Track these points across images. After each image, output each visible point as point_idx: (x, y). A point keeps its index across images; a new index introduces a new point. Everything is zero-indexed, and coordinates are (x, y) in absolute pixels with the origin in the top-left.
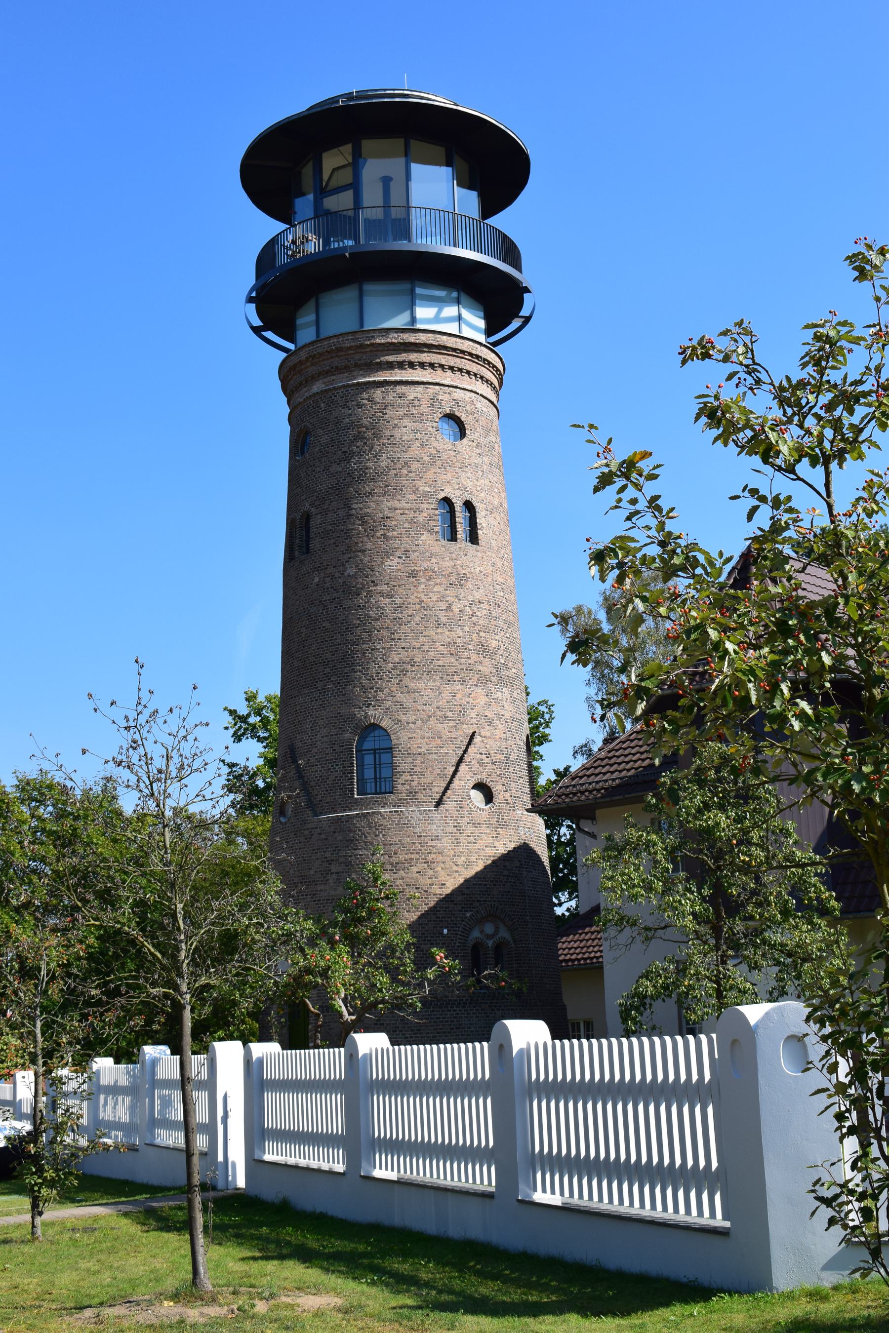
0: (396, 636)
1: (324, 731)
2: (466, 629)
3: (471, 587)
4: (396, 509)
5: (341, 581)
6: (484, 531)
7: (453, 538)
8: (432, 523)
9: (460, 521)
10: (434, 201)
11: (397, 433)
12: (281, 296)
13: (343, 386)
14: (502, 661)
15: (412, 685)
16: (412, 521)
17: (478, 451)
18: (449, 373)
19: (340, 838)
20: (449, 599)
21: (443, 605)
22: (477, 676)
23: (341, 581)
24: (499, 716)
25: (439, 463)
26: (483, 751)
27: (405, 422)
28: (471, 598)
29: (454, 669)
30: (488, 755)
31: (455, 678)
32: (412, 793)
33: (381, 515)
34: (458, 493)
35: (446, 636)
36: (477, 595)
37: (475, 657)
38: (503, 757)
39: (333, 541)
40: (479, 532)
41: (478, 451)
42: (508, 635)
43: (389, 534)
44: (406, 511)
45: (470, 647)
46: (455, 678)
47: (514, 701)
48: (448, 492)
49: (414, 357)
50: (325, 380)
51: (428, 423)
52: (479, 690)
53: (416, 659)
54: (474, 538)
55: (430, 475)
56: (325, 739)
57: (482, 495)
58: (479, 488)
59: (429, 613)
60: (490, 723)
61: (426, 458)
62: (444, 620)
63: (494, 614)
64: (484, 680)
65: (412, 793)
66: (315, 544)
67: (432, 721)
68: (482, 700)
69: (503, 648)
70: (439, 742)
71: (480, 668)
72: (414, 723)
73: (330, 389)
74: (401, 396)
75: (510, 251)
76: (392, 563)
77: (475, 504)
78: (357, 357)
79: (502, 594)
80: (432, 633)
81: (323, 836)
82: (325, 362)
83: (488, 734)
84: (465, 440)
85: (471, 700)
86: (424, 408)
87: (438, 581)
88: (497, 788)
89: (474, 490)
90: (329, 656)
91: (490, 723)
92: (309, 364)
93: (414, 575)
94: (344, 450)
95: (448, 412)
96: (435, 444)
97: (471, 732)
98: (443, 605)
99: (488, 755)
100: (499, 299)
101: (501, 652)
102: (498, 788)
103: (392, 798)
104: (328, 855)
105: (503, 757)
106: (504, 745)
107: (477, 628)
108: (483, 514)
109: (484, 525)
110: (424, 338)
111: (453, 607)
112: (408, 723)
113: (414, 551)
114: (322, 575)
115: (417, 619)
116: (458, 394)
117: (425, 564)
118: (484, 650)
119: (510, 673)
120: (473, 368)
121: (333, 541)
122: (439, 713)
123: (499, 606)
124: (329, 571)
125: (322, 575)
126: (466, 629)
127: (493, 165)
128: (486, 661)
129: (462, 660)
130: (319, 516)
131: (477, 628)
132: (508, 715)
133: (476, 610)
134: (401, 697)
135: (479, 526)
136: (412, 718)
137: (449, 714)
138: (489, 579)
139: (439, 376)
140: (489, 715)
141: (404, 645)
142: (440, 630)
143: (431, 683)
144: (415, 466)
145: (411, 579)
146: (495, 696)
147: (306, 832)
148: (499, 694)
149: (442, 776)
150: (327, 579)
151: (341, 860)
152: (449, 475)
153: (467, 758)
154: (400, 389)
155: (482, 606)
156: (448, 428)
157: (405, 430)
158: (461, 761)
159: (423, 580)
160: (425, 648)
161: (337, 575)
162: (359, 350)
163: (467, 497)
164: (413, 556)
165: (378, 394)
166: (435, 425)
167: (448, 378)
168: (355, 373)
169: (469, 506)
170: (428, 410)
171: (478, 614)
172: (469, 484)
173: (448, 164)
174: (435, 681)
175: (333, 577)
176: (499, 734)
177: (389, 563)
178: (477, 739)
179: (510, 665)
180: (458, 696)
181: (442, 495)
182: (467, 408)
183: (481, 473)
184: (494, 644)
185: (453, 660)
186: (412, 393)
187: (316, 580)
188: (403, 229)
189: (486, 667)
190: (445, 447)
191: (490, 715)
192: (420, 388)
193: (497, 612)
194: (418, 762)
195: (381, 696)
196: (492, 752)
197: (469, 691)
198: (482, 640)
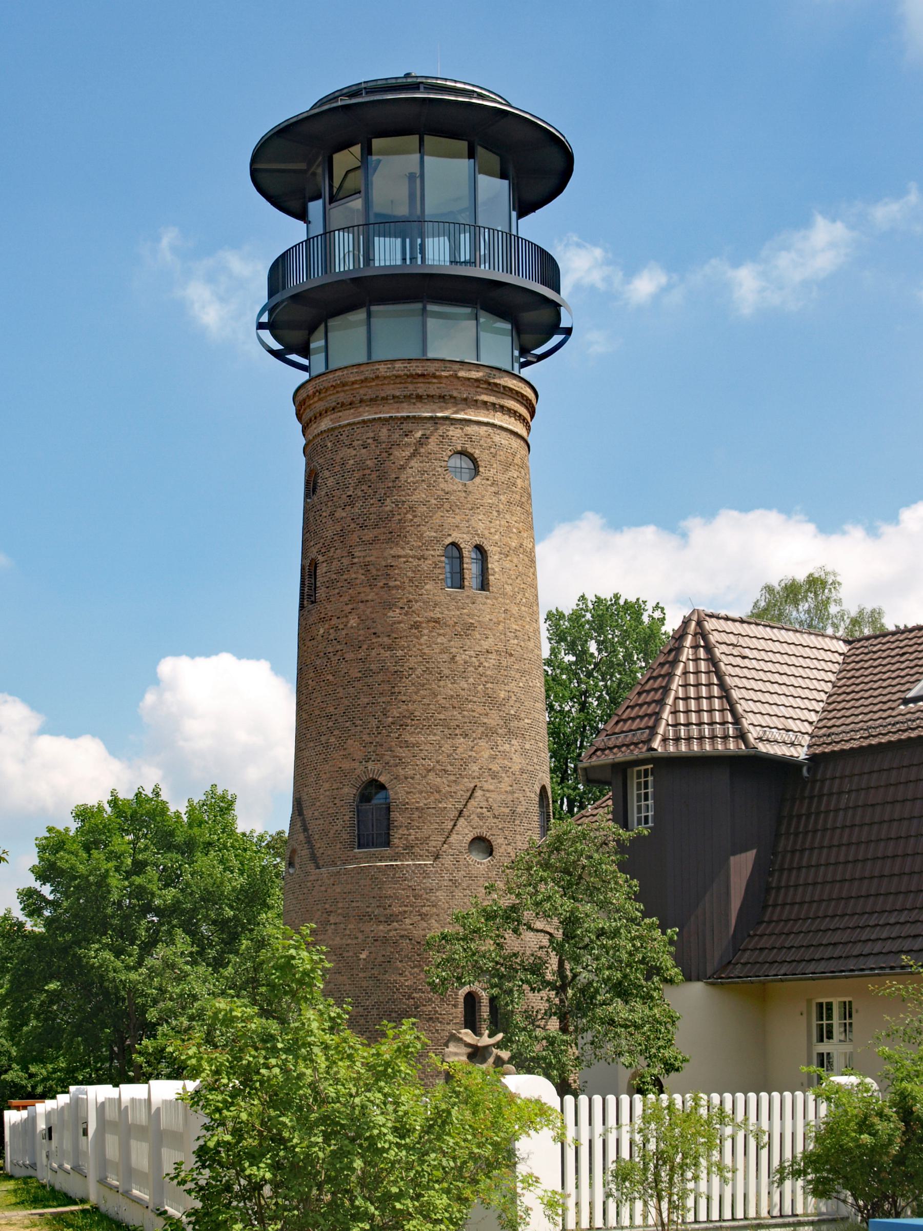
0: (396, 689)
1: (327, 786)
2: (471, 680)
3: (478, 636)
4: (399, 557)
5: (344, 632)
6: (497, 576)
7: (460, 584)
8: (438, 571)
13: (349, 424)
14: (512, 712)
17: (493, 489)
19: (338, 890)
20: (453, 650)
21: (446, 657)
22: (481, 729)
23: (344, 632)
24: (506, 769)
25: (447, 506)
26: (484, 804)
28: (478, 648)
29: (457, 723)
30: (490, 809)
31: (457, 732)
32: (409, 847)
33: (384, 563)
35: (449, 688)
36: (486, 645)
37: (480, 709)
38: (507, 810)
39: (337, 591)
40: (491, 578)
41: (493, 489)
42: (521, 684)
43: (391, 584)
44: (410, 559)
45: (475, 699)
46: (457, 732)
48: (456, 536)
50: (332, 417)
51: (436, 463)
53: (417, 714)
54: (484, 585)
55: (436, 520)
56: (328, 793)
57: (497, 537)
58: (493, 530)
59: (431, 665)
60: (494, 776)
61: (434, 501)
62: (447, 672)
63: (504, 664)
65: (409, 847)
66: (321, 593)
67: (431, 776)
68: (486, 754)
69: (514, 698)
71: (486, 720)
72: (412, 778)
73: (336, 428)
78: (362, 391)
79: (516, 641)
81: (323, 888)
82: (332, 397)
83: (492, 787)
84: (478, 480)
85: (474, 754)
87: (442, 631)
88: (498, 841)
89: (486, 532)
90: (332, 709)
91: (494, 776)
92: (316, 399)
93: (416, 626)
94: (349, 493)
95: (459, 449)
97: (472, 785)
98: (446, 657)
99: (490, 809)
101: (511, 702)
102: (499, 841)
103: (388, 851)
104: (327, 906)
105: (507, 810)
106: (510, 798)
107: (483, 679)
108: (496, 557)
109: (497, 570)
111: (457, 658)
112: (406, 778)
113: (417, 601)
114: (327, 626)
115: (419, 671)
118: (491, 701)
119: (521, 724)
121: (337, 591)
122: (438, 767)
123: (511, 655)
124: (333, 622)
125: (327, 626)
126: (471, 680)
128: (494, 713)
129: (465, 713)
130: (325, 564)
131: (483, 679)
132: (516, 768)
133: (482, 660)
134: (400, 752)
135: (490, 571)
137: (449, 768)
138: (501, 627)
140: (494, 769)
141: (404, 698)
142: (442, 683)
143: (432, 737)
144: (422, 509)
145: (414, 631)
146: (500, 748)
147: (309, 884)
150: (331, 631)
151: (340, 911)
155: (490, 656)
159: (426, 631)
160: (426, 701)
161: (341, 627)
162: (364, 385)
163: (477, 541)
164: (416, 606)
166: (443, 464)
168: (361, 409)
169: (479, 548)
171: (486, 664)
172: (481, 527)
174: (435, 735)
175: (337, 629)
176: (504, 786)
177: (391, 614)
178: (478, 793)
179: (522, 716)
180: (459, 750)
181: (449, 540)
182: (482, 442)
183: (495, 514)
184: (502, 695)
185: (455, 713)
187: (322, 631)
189: (494, 719)
190: (455, 488)
191: (495, 767)
196: (495, 806)
197: (471, 744)
198: (490, 691)
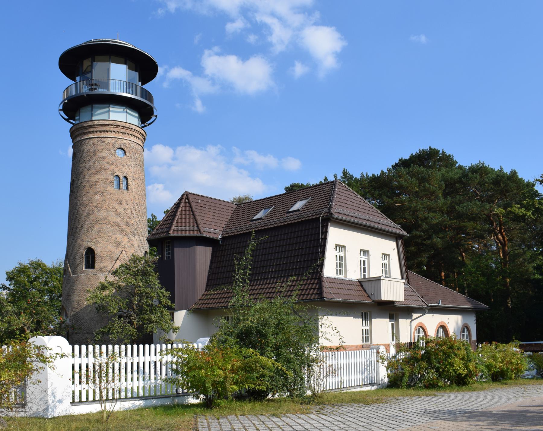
9: (122, 181)
10: (118, 77)
11: (101, 154)
12: (73, 107)
15: (102, 235)
16: (105, 183)
18: (103, 133)
21: (114, 210)
25: (115, 164)
27: (104, 151)
34: (121, 174)
35: (115, 220)
36: (127, 207)
37: (125, 226)
47: (139, 240)
48: (118, 173)
49: (108, 129)
52: (125, 237)
54: (127, 189)
60: (129, 247)
62: (114, 214)
64: (127, 234)
67: (108, 247)
68: (127, 240)
70: (110, 253)
74: (103, 142)
75: (149, 96)
76: (98, 196)
77: (128, 177)
80: (110, 219)
86: (111, 146)
91: (129, 247)
93: (105, 200)
96: (114, 158)
100: (145, 111)
110: (111, 123)
116: (124, 141)
117: (108, 197)
118: (128, 224)
120: (130, 132)
127: (145, 67)
128: (129, 228)
132: (136, 245)
136: (102, 245)
139: (103, 135)
143: (109, 235)
148: (133, 238)
149: (111, 264)
152: (119, 168)
153: (119, 258)
154: (103, 140)
156: (121, 152)
157: (104, 153)
158: (118, 259)
164: (105, 194)
165: (96, 141)
167: (120, 136)
169: (126, 177)
170: (112, 147)
172: (126, 171)
173: (125, 64)
178: (124, 252)
184: (132, 222)
186: (107, 141)
188: (107, 87)
192: (110, 139)
193: (134, 212)
194: (103, 259)
195: (92, 238)
